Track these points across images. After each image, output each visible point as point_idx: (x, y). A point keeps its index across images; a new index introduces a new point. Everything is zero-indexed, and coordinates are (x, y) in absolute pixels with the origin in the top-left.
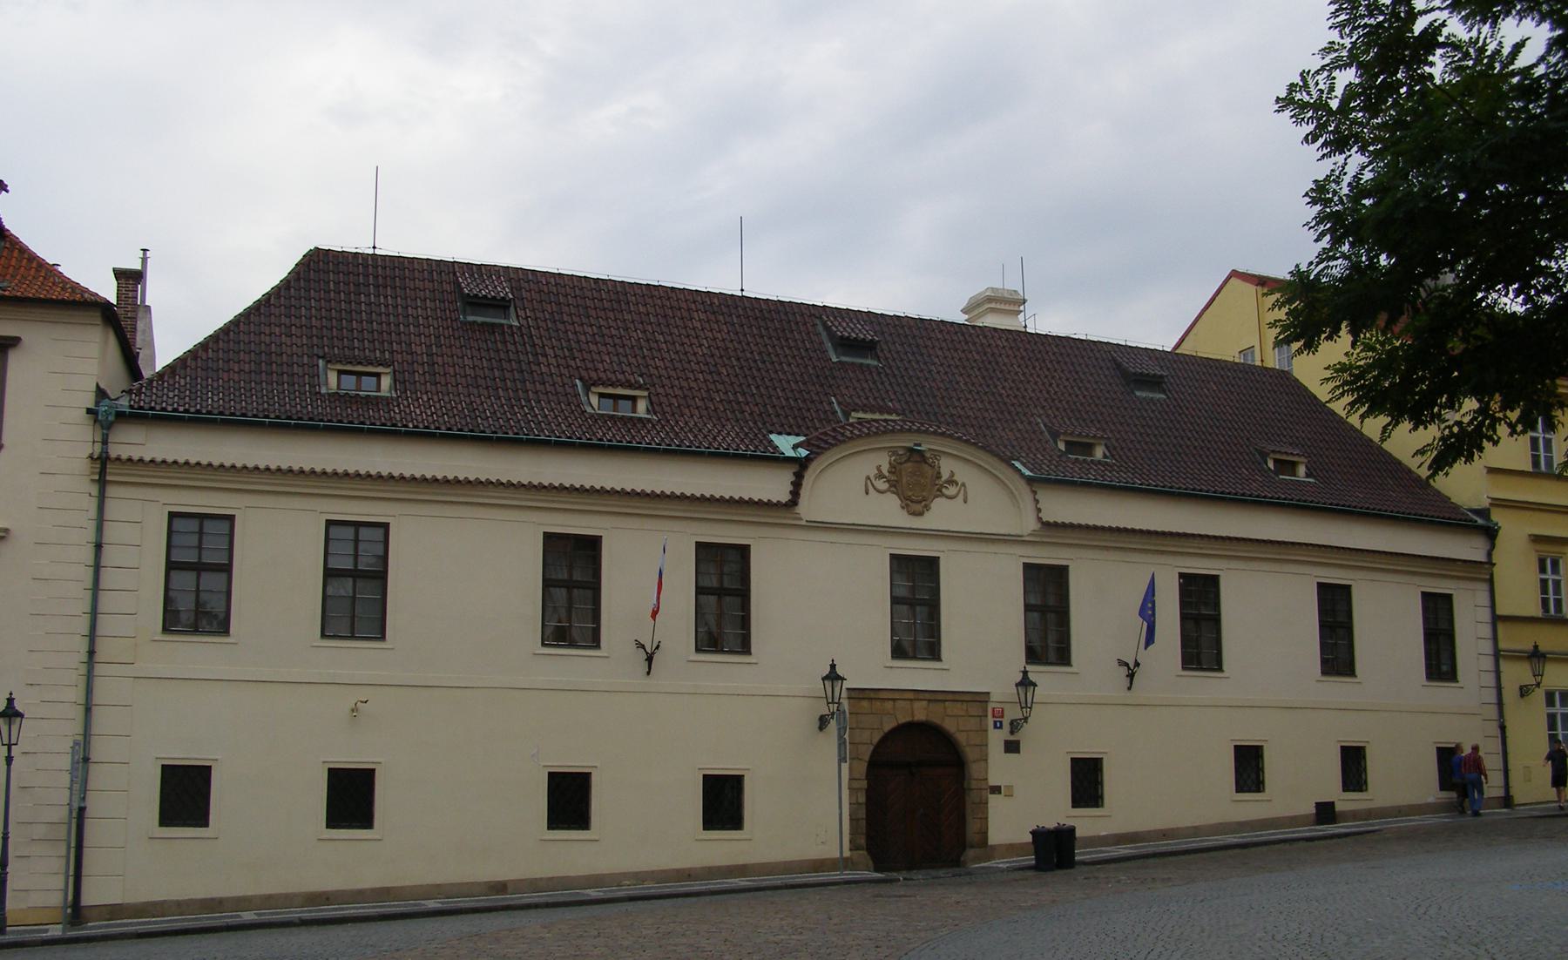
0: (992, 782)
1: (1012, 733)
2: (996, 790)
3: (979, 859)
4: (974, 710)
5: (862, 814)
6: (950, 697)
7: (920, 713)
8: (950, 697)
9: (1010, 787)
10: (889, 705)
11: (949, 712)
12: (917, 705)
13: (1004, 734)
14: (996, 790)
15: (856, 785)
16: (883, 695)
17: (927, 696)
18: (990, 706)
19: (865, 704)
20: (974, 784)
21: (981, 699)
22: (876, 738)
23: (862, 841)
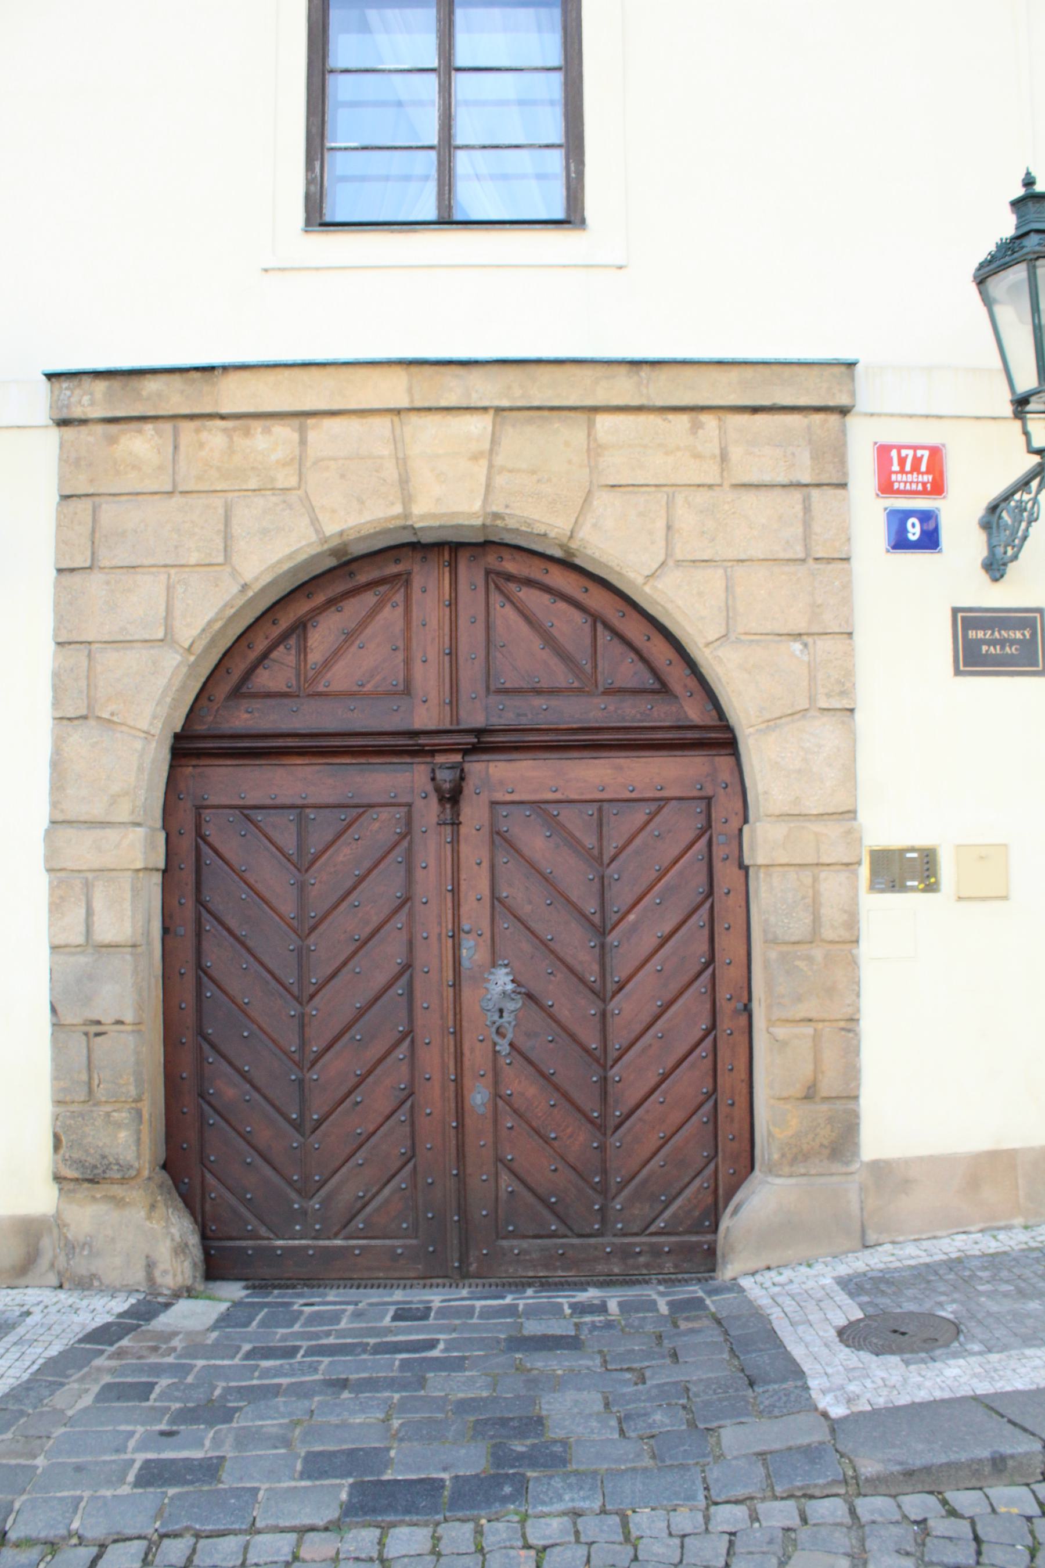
0: (884, 828)
1: (995, 567)
2: (908, 870)
3: (792, 1235)
4: (767, 450)
5: (128, 995)
6: (622, 389)
7: (448, 483)
8: (622, 389)
9: (991, 856)
10: (273, 443)
11: (616, 466)
12: (428, 434)
13: (955, 573)
14: (908, 870)
15: (83, 850)
16: (234, 395)
17: (484, 388)
18: (862, 440)
19: (141, 445)
20: (765, 841)
21: (815, 397)
22: (206, 610)
23: (129, 1138)
